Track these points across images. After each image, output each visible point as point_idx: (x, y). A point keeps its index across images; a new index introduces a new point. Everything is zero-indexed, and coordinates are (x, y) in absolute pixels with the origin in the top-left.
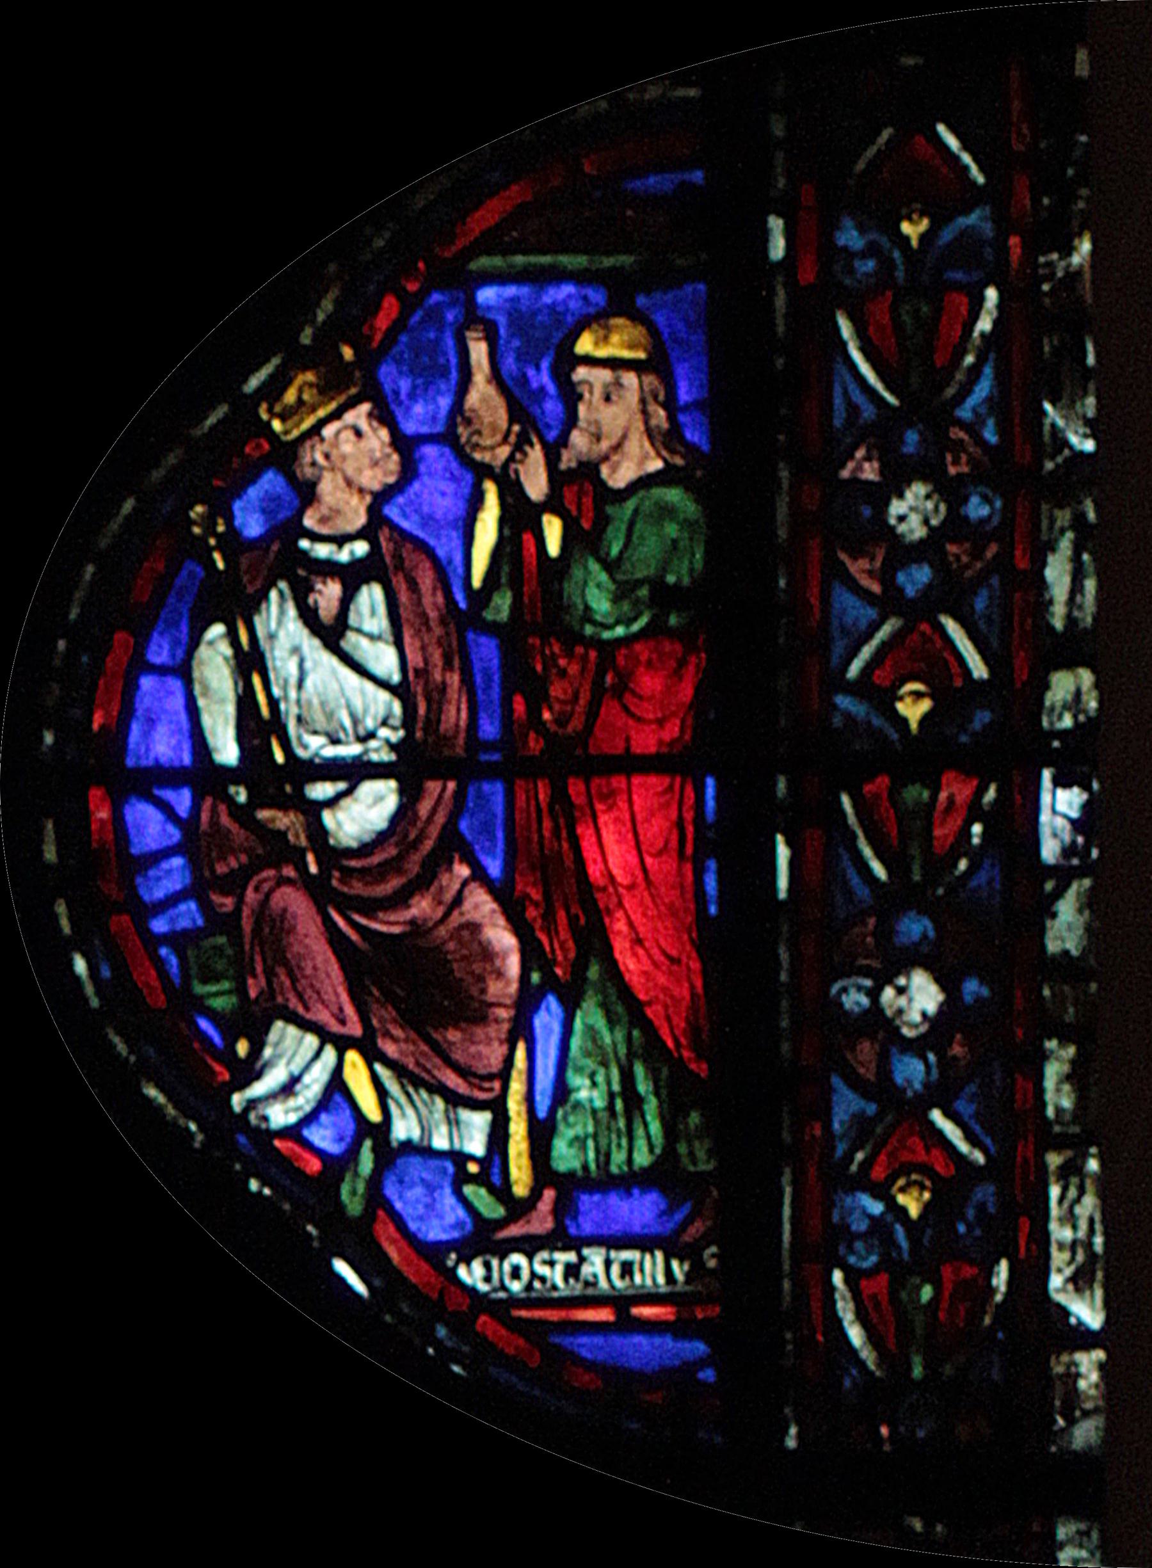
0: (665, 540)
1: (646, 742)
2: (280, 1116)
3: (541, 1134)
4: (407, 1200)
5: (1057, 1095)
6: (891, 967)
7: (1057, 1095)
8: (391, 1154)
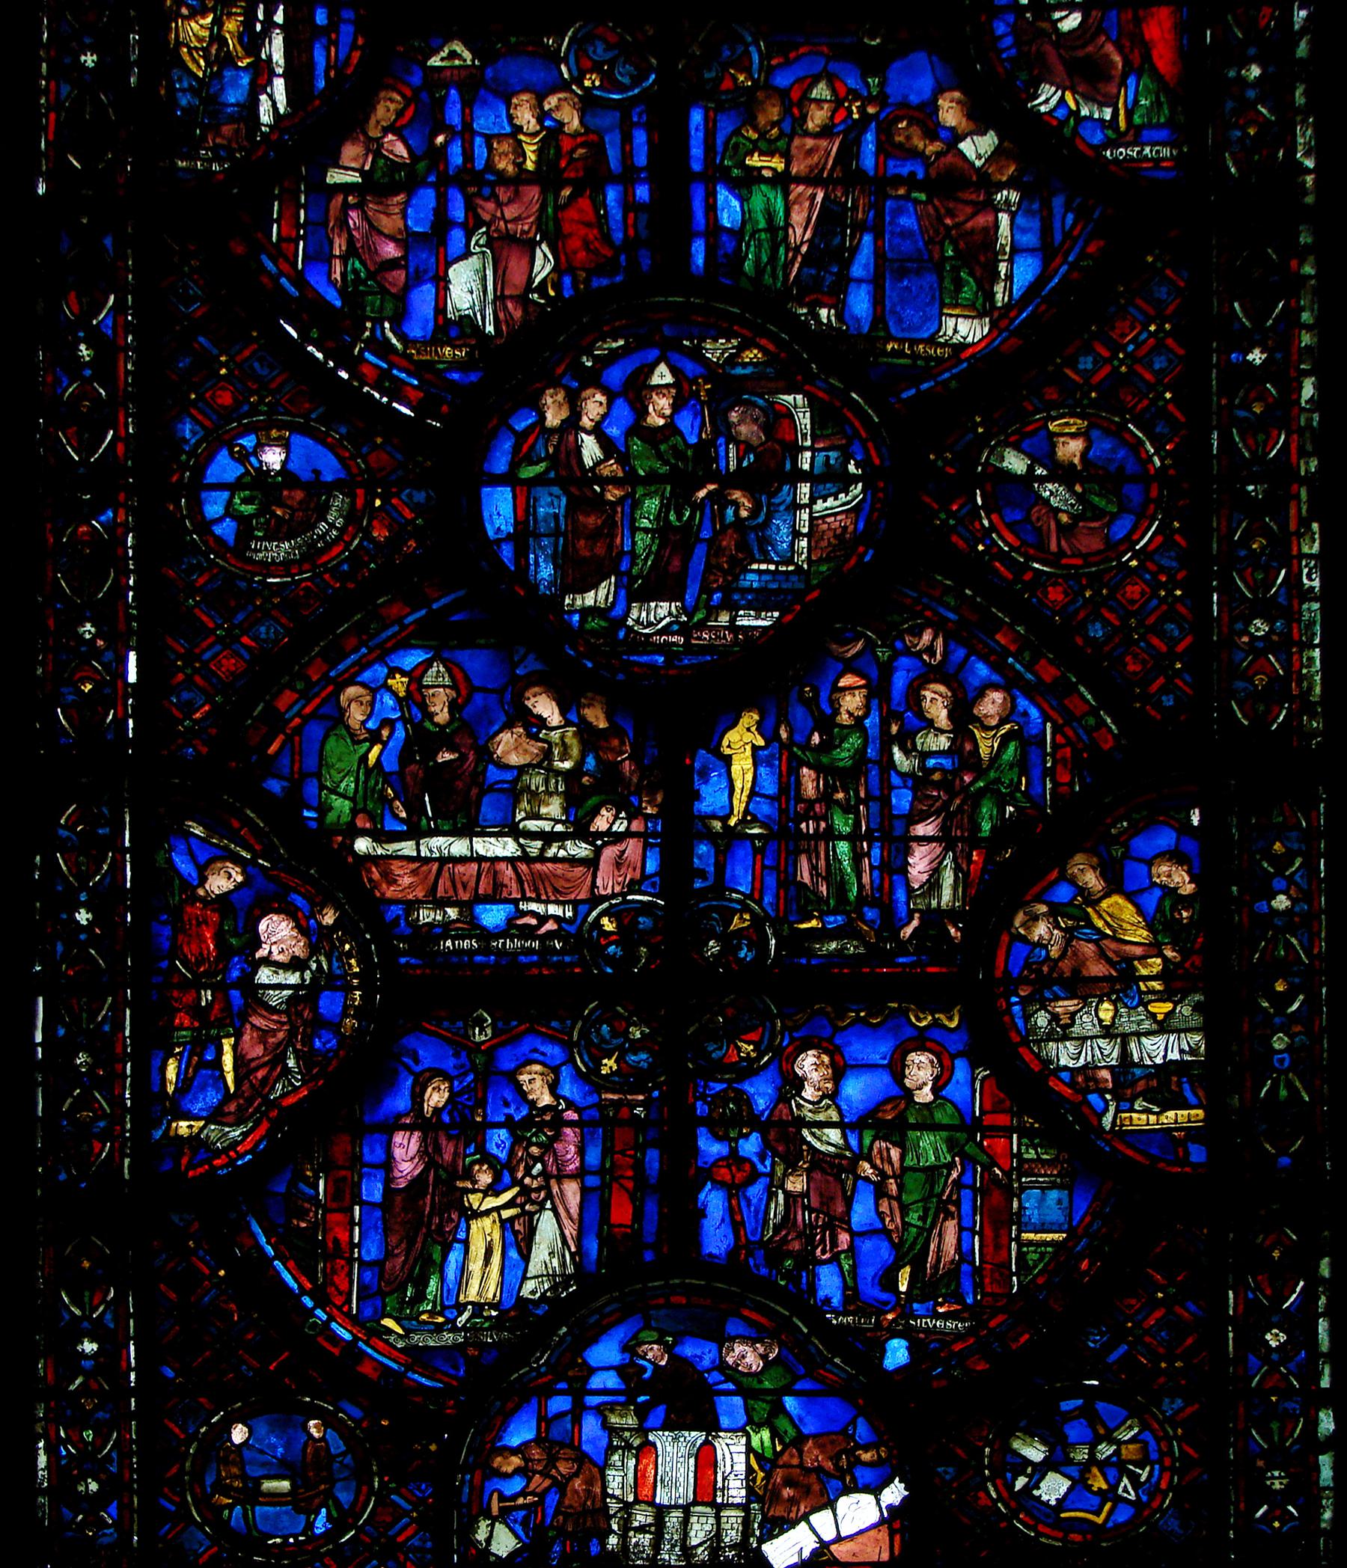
2: (1043, 109)
3: (1129, 114)
4: (1085, 132)
5: (1299, 98)
6: (1246, 63)
7: (1299, 98)
8: (1080, 120)
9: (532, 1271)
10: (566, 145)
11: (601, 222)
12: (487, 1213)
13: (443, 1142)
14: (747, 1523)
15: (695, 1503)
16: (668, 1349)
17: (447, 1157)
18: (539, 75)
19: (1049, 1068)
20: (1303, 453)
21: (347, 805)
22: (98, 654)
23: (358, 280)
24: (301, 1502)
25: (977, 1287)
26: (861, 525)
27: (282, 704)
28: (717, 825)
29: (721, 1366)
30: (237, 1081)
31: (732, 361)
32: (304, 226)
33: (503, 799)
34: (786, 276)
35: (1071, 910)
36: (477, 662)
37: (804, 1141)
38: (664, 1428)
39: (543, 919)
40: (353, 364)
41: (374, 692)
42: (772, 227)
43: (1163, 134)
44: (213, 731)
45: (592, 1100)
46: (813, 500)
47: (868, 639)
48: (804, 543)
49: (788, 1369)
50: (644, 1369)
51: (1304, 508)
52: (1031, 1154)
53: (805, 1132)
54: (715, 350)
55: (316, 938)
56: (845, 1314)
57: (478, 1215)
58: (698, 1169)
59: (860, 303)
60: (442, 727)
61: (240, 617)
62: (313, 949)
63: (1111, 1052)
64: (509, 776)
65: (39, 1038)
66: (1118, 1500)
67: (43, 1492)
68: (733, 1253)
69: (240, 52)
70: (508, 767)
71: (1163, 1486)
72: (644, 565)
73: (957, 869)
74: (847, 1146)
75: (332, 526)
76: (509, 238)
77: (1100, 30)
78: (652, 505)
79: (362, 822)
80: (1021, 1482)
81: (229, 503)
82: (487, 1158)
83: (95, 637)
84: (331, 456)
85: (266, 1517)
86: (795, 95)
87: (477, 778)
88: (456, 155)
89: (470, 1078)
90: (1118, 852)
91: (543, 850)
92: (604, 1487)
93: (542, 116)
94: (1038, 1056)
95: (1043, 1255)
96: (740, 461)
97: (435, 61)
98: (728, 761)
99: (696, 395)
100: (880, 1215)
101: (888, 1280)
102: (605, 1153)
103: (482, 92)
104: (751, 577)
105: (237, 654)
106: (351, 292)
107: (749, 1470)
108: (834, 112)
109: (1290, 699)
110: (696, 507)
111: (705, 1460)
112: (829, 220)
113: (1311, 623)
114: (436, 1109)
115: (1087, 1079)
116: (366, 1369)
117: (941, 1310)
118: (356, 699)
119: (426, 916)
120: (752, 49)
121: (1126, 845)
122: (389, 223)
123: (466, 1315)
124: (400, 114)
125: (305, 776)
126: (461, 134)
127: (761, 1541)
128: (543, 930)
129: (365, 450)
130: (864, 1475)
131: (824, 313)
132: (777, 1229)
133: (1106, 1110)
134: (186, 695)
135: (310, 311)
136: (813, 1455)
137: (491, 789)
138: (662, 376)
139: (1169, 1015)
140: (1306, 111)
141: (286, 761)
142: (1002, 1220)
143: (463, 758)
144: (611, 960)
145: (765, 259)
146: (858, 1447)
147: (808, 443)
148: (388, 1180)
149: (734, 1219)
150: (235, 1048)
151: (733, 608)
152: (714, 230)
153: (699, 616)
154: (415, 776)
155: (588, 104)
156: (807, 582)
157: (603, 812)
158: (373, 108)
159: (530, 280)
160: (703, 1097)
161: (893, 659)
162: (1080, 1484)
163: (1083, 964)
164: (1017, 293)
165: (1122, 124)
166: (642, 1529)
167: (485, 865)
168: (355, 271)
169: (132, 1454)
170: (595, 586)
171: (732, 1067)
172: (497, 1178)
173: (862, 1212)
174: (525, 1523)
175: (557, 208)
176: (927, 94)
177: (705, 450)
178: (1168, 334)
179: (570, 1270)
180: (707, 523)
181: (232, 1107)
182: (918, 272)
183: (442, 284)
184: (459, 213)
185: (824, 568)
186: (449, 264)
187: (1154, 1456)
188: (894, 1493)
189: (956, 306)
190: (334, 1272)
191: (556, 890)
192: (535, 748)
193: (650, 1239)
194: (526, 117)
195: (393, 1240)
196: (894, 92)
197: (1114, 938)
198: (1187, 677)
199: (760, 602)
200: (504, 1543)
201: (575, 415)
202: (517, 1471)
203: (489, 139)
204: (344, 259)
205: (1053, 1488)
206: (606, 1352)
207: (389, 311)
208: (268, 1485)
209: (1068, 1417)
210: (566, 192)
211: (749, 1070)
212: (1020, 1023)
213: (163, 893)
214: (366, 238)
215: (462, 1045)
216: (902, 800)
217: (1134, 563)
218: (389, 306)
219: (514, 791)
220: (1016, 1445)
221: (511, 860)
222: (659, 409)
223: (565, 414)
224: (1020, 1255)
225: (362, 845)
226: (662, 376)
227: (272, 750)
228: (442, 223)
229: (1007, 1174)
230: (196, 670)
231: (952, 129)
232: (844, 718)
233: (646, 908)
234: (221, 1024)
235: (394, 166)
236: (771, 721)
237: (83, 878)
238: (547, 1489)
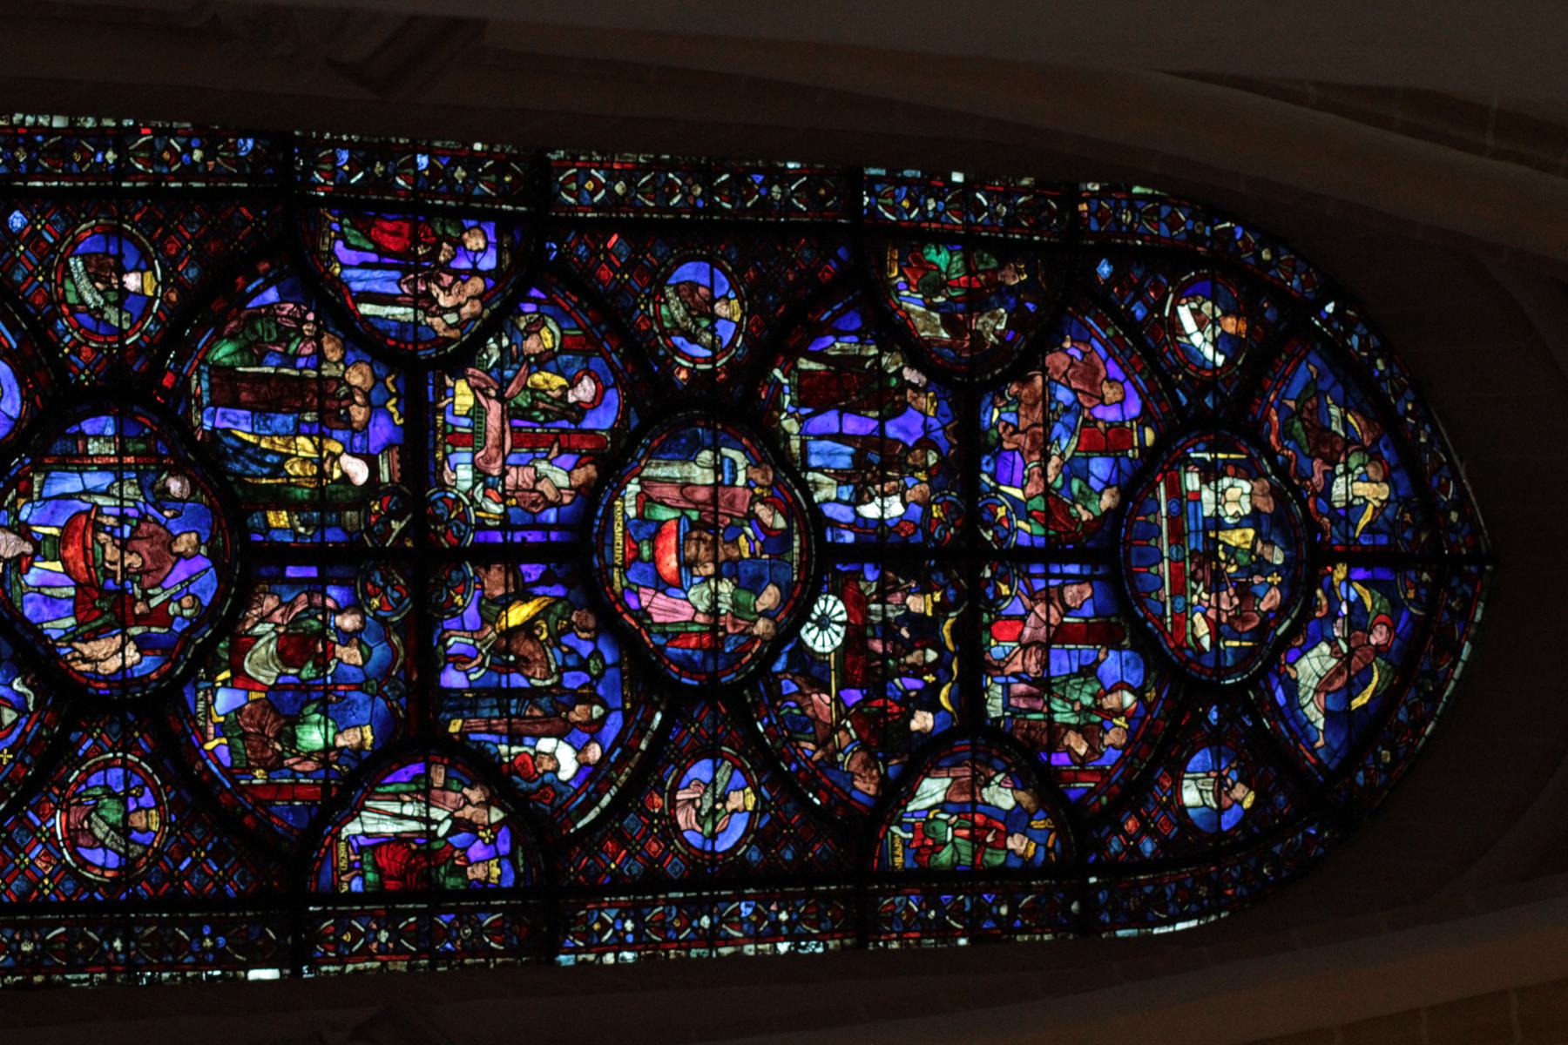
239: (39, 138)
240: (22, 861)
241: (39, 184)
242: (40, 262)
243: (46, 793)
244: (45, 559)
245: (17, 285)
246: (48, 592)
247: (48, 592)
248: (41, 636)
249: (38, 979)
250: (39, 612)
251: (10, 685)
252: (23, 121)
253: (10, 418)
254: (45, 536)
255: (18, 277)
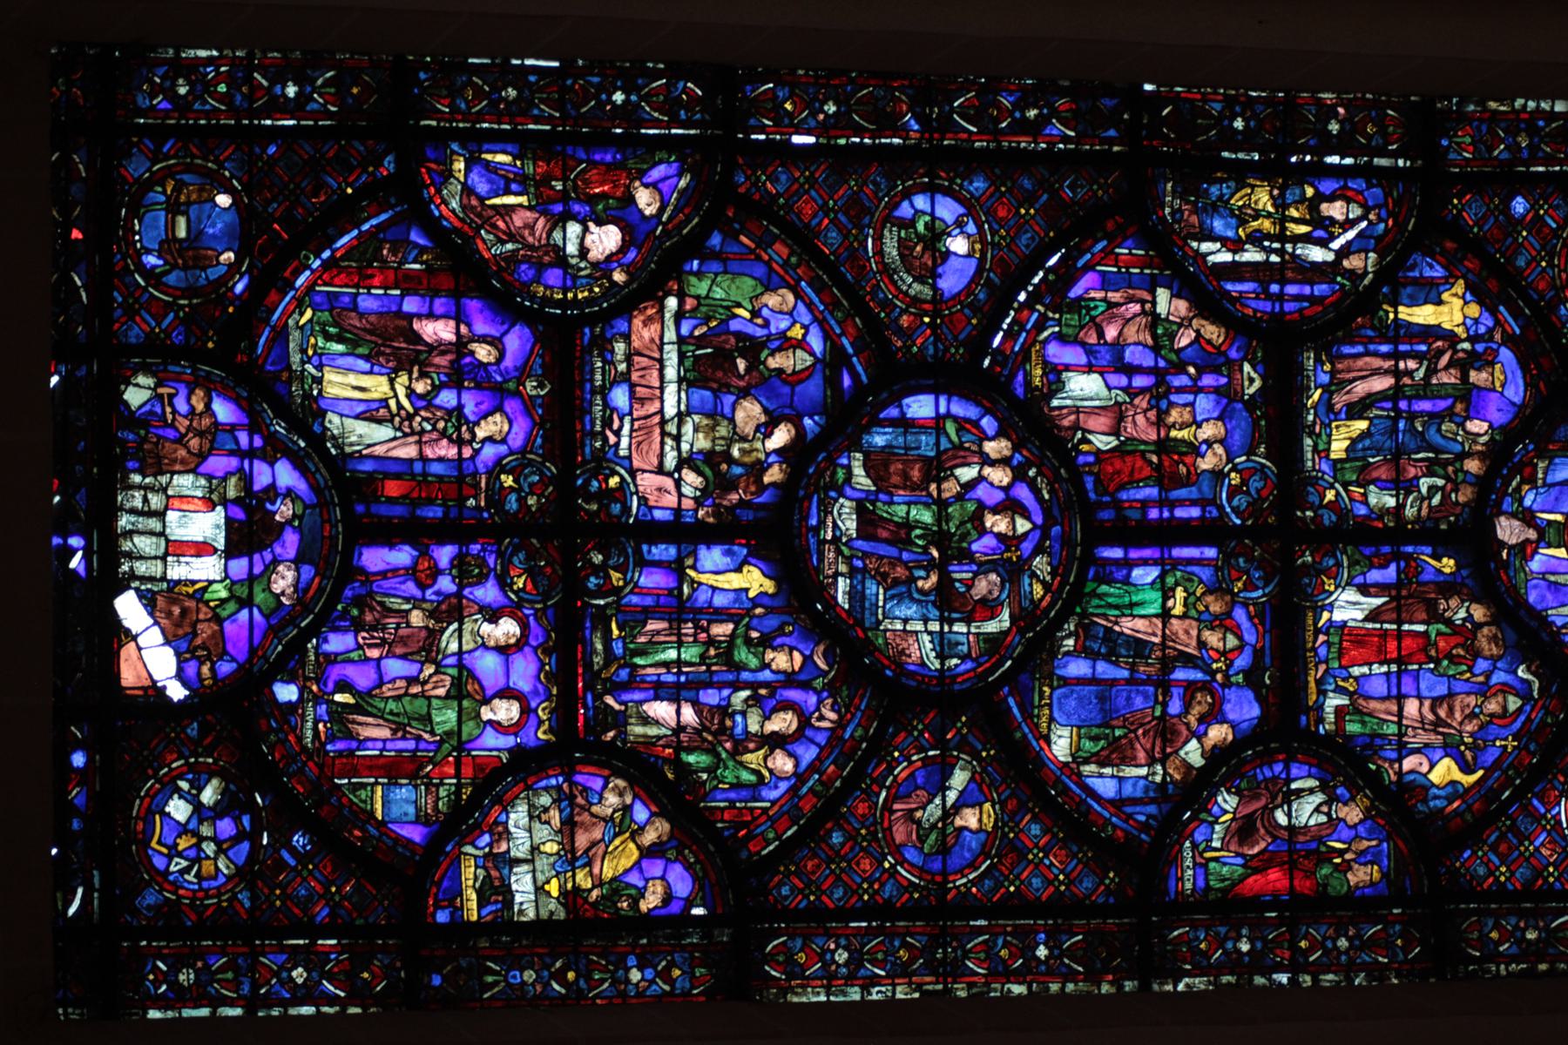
0: (1337, 887)
1: (1296, 882)
2: (1220, 799)
3: (1216, 859)
4: (1203, 829)
5: (1226, 979)
6: (1251, 940)
7: (1226, 979)
8: (1212, 824)
9: (349, 422)
10: (1188, 460)
11: (1133, 482)
12: (393, 389)
13: (449, 357)
14: (151, 579)
15: (168, 541)
16: (289, 522)
17: (437, 360)
18: (1238, 439)
19: (507, 806)
20: (970, 986)
21: (703, 292)
22: (813, 114)
23: (1089, 309)
24: (168, 246)
25: (340, 753)
26: (912, 668)
27: (777, 246)
28: (689, 562)
29: (276, 561)
30: (494, 207)
31: (1033, 575)
32: (1127, 272)
33: (709, 406)
34: (1097, 615)
35: (627, 821)
36: (813, 389)
37: (449, 624)
38: (227, 518)
39: (618, 433)
40: (1029, 305)
41: (790, 314)
42: (1132, 605)
43: (1201, 883)
44: (757, 197)
45: (481, 467)
46: (930, 633)
47: (827, 673)
48: (899, 626)
49: (274, 611)
50: (273, 503)
51: (930, 987)
52: (443, 793)
53: (455, 625)
54: (1041, 564)
55: (603, 268)
56: (317, 655)
57: (392, 382)
58: (428, 547)
59: (1078, 668)
60: (764, 363)
61: (843, 218)
62: (595, 265)
63: (520, 848)
64: (727, 410)
65: (529, 62)
66: (170, 858)
67: (177, 53)
68: (363, 571)
69: (1249, 230)
70: (734, 410)
71: (181, 892)
72: (882, 510)
73: (659, 738)
74: (445, 657)
75: (910, 286)
76: (1121, 418)
77: (1275, 838)
78: (927, 517)
79: (690, 303)
80: (184, 785)
81: (924, 213)
82: (437, 389)
83: (825, 113)
84: (961, 286)
85: (156, 219)
86: (1228, 622)
87: (725, 387)
88: (1180, 381)
89: (499, 379)
90: (671, 854)
91: (669, 435)
92: (179, 472)
93: (1209, 443)
94: (517, 797)
95: (365, 802)
96: (960, 581)
97: (1247, 367)
98: (738, 570)
99: (1008, 550)
100: (393, 680)
101: (344, 686)
102: (440, 477)
103: (1225, 401)
104: (874, 588)
105: (815, 215)
106: (1078, 305)
107: (194, 582)
108: (1217, 650)
109: (788, 979)
110: (925, 549)
111: (202, 549)
112: (1138, 647)
113: (845, 994)
114: (472, 353)
115: (500, 834)
116: (273, 296)
117: (321, 726)
118: (784, 301)
119: (620, 347)
120: (1260, 592)
121: (676, 860)
122: (1131, 333)
123: (313, 371)
124: (1209, 342)
125: (725, 261)
126: (1195, 385)
127: (137, 590)
128: (609, 433)
129: (967, 311)
130: (191, 668)
131: (1071, 642)
132: (382, 604)
133: (477, 848)
134: (783, 178)
135: (1067, 274)
136: (206, 630)
137: (716, 397)
138: (1023, 526)
139: (548, 894)
140: (1216, 983)
141: (736, 249)
142: (394, 769)
143: (741, 377)
144: (587, 483)
145: (1110, 600)
146: (213, 664)
147: (973, 630)
148: (420, 316)
149: (391, 572)
150: (520, 205)
151: (852, 573)
152: (1129, 564)
153: (846, 550)
154: (727, 341)
155: (1218, 475)
156: (871, 629)
157: (700, 479)
158: (1213, 323)
159: (1090, 432)
160: (484, 550)
161: (815, 690)
162: (183, 829)
163: (586, 830)
164: (1089, 781)
165: (1208, 855)
166: (145, 500)
167: (657, 392)
168: (1096, 307)
169: (209, 119)
170: (868, 475)
171: (505, 571)
172: (421, 397)
173: (394, 667)
174: (151, 413)
175: (1143, 453)
176: (1231, 716)
177: (967, 556)
178: (1057, 888)
179: (348, 450)
180: (913, 557)
181: (474, 202)
182: (1102, 709)
183: (1089, 369)
184: (1139, 381)
185: (880, 641)
186: (1102, 374)
187: (205, 884)
188: (177, 692)
189: (1080, 738)
190: (349, 274)
191: (640, 443)
192: (749, 430)
193: (374, 509)
194: (1208, 431)
195: (373, 318)
196: (1231, 694)
197: (606, 853)
198: (802, 905)
199: (856, 595)
200: (135, 396)
201: (993, 463)
202: (193, 409)
203: (1192, 404)
204: (1104, 300)
205: (179, 809)
206: (286, 475)
207: (1065, 330)
208: (182, 222)
209: (237, 820)
210: (1155, 459)
211: (504, 583)
212: (543, 783)
213: (639, 154)
214: (1122, 316)
215: (523, 372)
216: (711, 697)
217: (887, 865)
218: (1070, 331)
219: (714, 415)
220: (215, 782)
221: (661, 411)
222: (998, 523)
223: (994, 455)
224: (363, 786)
225: (672, 303)
226: (1023, 526)
227: (743, 239)
228: (1131, 370)
229: (428, 775)
230: (802, 185)
231: (1206, 734)
232: (770, 655)
233: (626, 509)
234: (537, 197)
235: (1172, 337)
236: (766, 601)
237: (646, 98)
238: (177, 430)
239: (1541, 123)
240: (1527, 849)
241: (1541, 169)
242: (1543, 248)
243: (1551, 781)
244: (1549, 546)
245: (1520, 271)
246: (1552, 578)
247: (1552, 578)
248: (1545, 622)
249: (1543, 967)
250: (1543, 598)
251: (1515, 672)
252: (1525, 106)
253: (1513, 404)
254: (1550, 522)
255: (1521, 262)
